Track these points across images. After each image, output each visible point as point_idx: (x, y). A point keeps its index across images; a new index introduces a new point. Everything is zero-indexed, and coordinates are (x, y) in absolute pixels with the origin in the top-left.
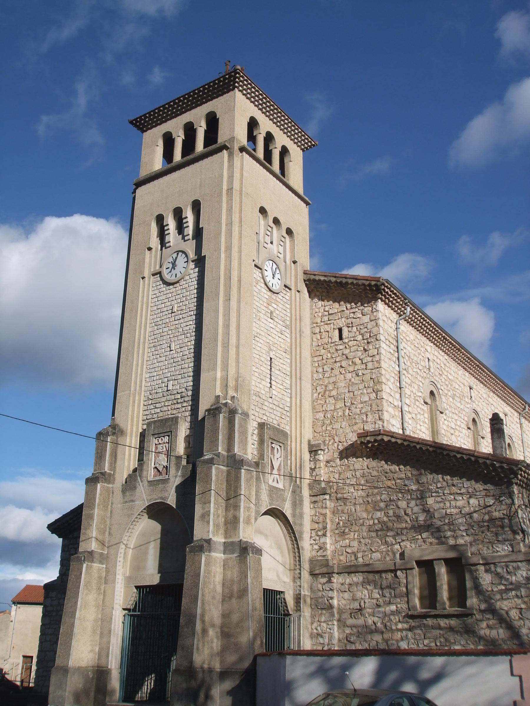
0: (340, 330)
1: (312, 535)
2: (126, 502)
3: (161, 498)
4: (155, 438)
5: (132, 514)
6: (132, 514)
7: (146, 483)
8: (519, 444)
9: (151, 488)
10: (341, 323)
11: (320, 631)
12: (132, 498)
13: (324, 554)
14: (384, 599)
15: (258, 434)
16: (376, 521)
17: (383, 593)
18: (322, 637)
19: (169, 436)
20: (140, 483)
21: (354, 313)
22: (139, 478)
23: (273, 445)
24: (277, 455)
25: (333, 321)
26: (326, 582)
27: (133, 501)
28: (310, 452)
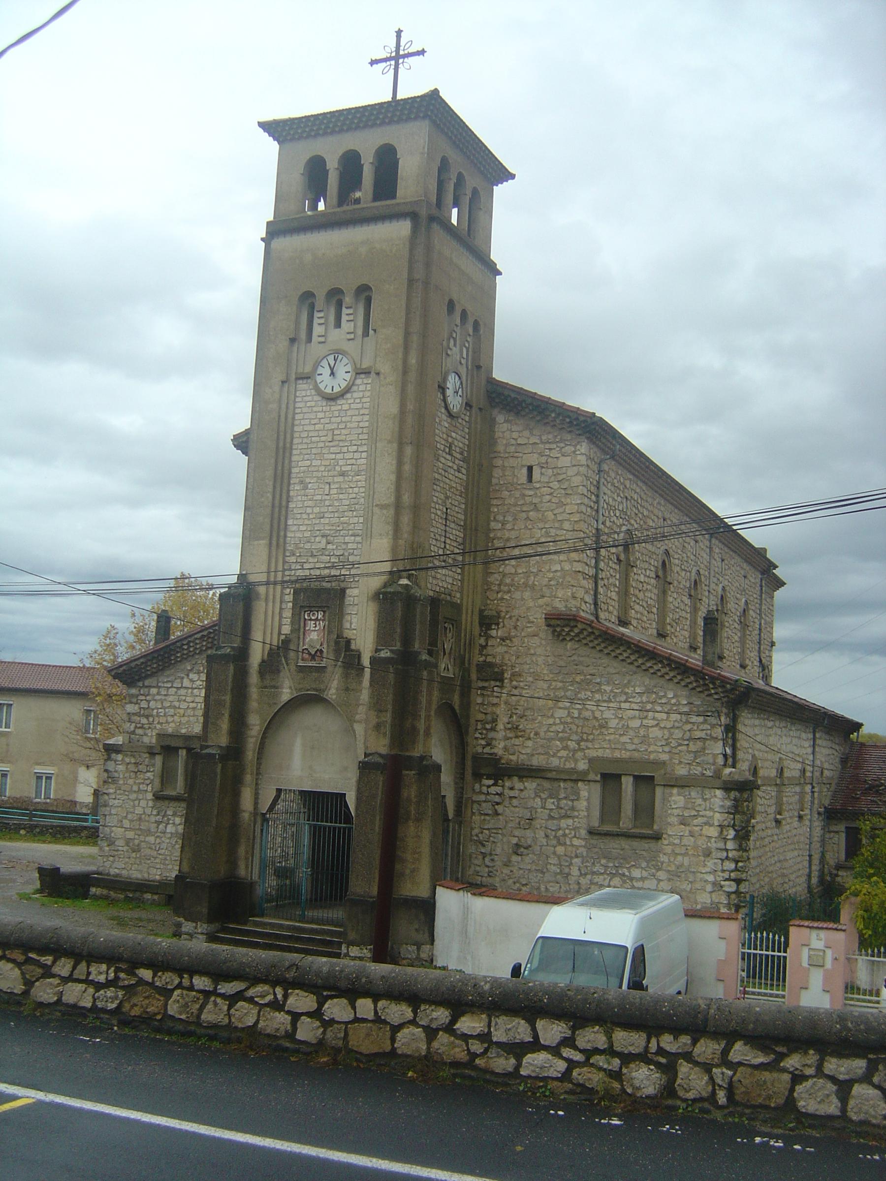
0: (530, 469)
1: (479, 728)
2: (266, 687)
3: (316, 690)
4: (305, 612)
5: (275, 704)
6: (275, 704)
7: (293, 667)
8: (705, 576)
9: (301, 674)
10: (533, 459)
11: (481, 838)
12: (273, 683)
13: (493, 751)
14: (560, 811)
15: (770, 1012)
16: (558, 721)
17: (558, 804)
18: (484, 845)
19: (324, 612)
20: (286, 667)
21: (550, 449)
22: (283, 659)
23: (446, 625)
24: (449, 635)
25: (521, 455)
26: (493, 785)
27: (276, 687)
28: (481, 624)
